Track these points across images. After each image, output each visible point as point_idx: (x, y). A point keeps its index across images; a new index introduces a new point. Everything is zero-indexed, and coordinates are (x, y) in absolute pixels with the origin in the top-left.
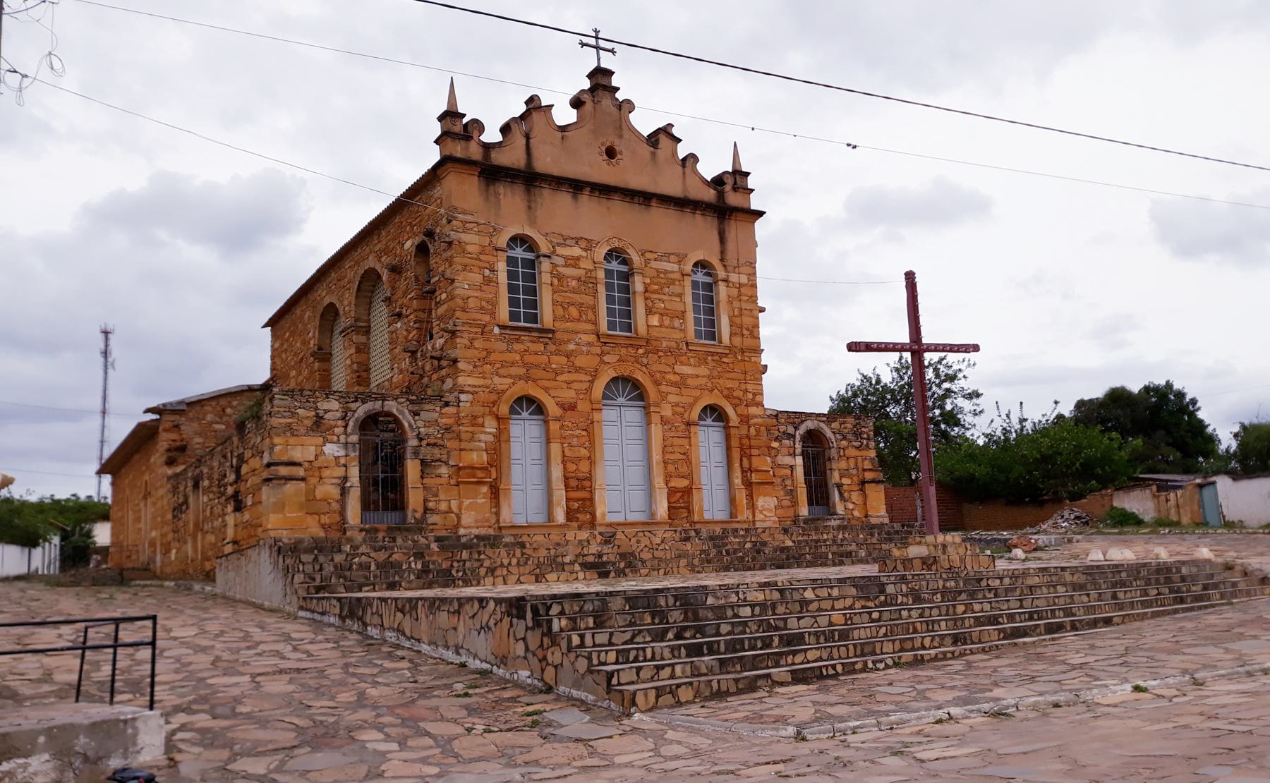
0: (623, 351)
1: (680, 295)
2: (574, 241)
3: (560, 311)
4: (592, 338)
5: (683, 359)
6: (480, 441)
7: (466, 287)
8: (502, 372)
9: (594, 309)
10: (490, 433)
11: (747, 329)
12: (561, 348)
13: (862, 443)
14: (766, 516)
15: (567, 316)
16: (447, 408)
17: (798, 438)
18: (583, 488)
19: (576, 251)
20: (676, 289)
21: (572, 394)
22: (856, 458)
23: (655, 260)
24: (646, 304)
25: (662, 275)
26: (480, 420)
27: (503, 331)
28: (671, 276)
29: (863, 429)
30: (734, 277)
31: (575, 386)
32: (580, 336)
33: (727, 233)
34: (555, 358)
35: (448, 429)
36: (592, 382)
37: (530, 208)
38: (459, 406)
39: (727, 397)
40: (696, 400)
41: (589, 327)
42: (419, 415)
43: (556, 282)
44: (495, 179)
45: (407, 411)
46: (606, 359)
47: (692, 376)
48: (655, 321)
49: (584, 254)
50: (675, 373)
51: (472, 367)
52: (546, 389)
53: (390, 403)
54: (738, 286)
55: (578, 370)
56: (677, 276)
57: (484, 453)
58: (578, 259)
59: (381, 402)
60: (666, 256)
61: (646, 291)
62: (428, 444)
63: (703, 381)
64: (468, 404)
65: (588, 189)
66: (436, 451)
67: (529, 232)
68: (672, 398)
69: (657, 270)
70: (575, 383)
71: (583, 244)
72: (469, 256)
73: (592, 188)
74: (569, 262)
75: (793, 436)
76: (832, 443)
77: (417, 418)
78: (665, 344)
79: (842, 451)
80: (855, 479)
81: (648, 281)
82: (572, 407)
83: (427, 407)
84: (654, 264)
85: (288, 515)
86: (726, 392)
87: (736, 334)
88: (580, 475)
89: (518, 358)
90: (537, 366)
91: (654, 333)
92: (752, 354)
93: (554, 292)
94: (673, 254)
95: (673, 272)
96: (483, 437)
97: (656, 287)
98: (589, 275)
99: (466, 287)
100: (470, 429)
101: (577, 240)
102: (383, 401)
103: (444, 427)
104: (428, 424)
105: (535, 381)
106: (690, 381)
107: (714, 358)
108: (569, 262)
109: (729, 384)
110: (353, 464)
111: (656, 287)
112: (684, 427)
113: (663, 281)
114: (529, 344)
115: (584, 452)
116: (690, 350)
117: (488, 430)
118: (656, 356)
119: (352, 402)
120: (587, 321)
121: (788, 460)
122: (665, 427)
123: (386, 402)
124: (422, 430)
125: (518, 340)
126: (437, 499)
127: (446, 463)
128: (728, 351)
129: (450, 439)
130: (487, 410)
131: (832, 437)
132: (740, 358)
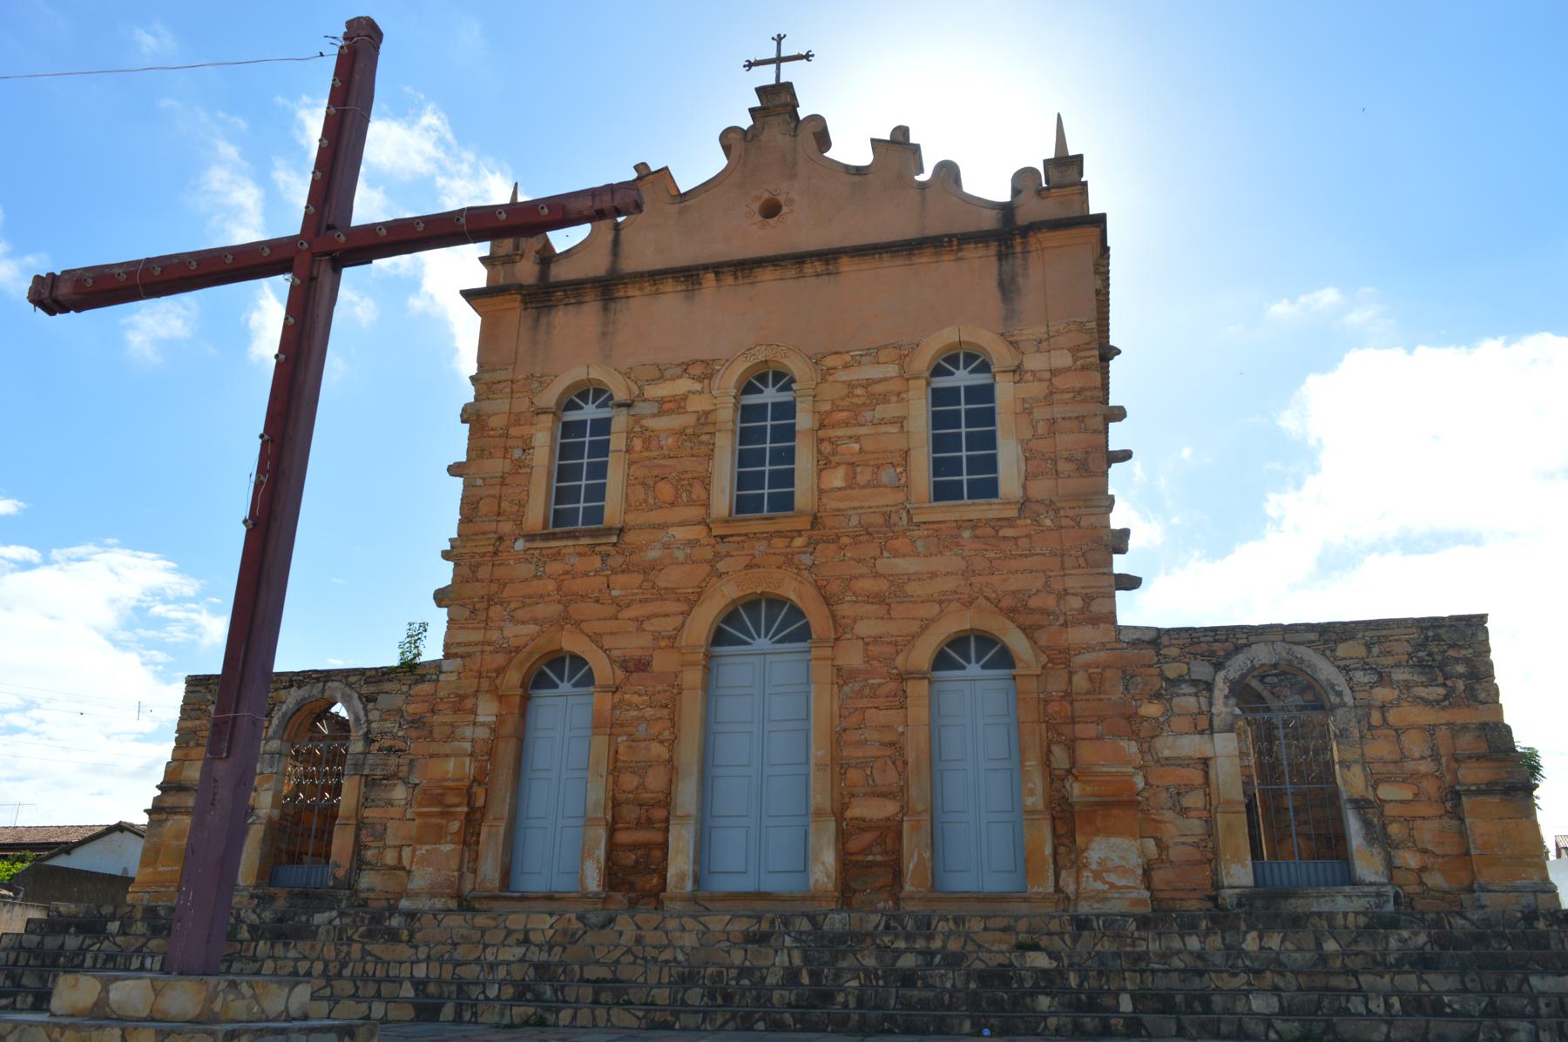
0: (761, 546)
1: (900, 421)
2: (679, 370)
3: (640, 492)
4: (697, 532)
5: (897, 544)
6: (463, 739)
7: (479, 482)
8: (520, 614)
9: (706, 480)
10: (483, 724)
11: (1068, 460)
12: (635, 558)
13: (1453, 689)
14: (1112, 886)
15: (651, 501)
16: (420, 686)
17: (1221, 689)
18: (649, 823)
19: (684, 385)
20: (891, 410)
21: (644, 641)
22: (1431, 730)
23: (846, 367)
24: (819, 451)
25: (859, 391)
26: (469, 703)
27: (529, 545)
28: (879, 388)
29: (1451, 653)
30: (1035, 362)
31: (652, 626)
32: (672, 531)
33: (1020, 280)
34: (621, 579)
35: (417, 722)
36: (686, 614)
37: (604, 334)
38: (437, 680)
39: (1011, 613)
40: (926, 624)
41: (695, 512)
42: (375, 700)
43: (638, 444)
44: (549, 307)
45: (356, 696)
46: (722, 566)
47: (918, 577)
48: (836, 479)
49: (697, 386)
50: (877, 575)
51: (467, 613)
52: (596, 639)
53: (336, 684)
54: (1047, 375)
55: (662, 594)
56: (894, 386)
57: (467, 760)
58: (685, 398)
59: (321, 685)
60: (873, 354)
61: (822, 426)
62: (380, 749)
63: (950, 584)
64: (454, 677)
65: (711, 276)
66: (393, 760)
67: (596, 373)
68: (866, 628)
69: (851, 385)
70: (654, 621)
71: (697, 370)
72: (491, 433)
73: (717, 274)
74: (667, 406)
75: (1209, 687)
76: (1339, 694)
77: (370, 706)
78: (854, 521)
79: (1376, 717)
80: (1430, 787)
81: (826, 407)
82: (642, 665)
83: (387, 686)
84: (843, 376)
85: (161, 869)
86: (1007, 602)
87: (1035, 476)
88: (646, 796)
89: (551, 586)
90: (583, 597)
91: (832, 504)
92: (1083, 511)
93: (631, 463)
94: (886, 347)
95: (886, 379)
96: (468, 732)
97: (844, 415)
98: (702, 420)
99: (479, 482)
100: (448, 719)
101: (686, 367)
102: (326, 682)
103: (410, 719)
104: (387, 713)
105: (577, 624)
106: (913, 588)
107: (979, 532)
108: (667, 406)
109: (1015, 583)
110: (266, 786)
111: (844, 415)
112: (892, 686)
113: (860, 401)
114: (574, 560)
115: (658, 750)
116: (918, 525)
117: (480, 719)
118: (833, 547)
119: (285, 688)
120: (691, 503)
121: (1191, 745)
122: (846, 688)
123: (330, 684)
124: (374, 725)
125: (557, 555)
126: (381, 844)
127: (405, 782)
128: (1013, 513)
129: (418, 738)
130: (485, 683)
131: (1340, 681)
132: (1048, 522)
